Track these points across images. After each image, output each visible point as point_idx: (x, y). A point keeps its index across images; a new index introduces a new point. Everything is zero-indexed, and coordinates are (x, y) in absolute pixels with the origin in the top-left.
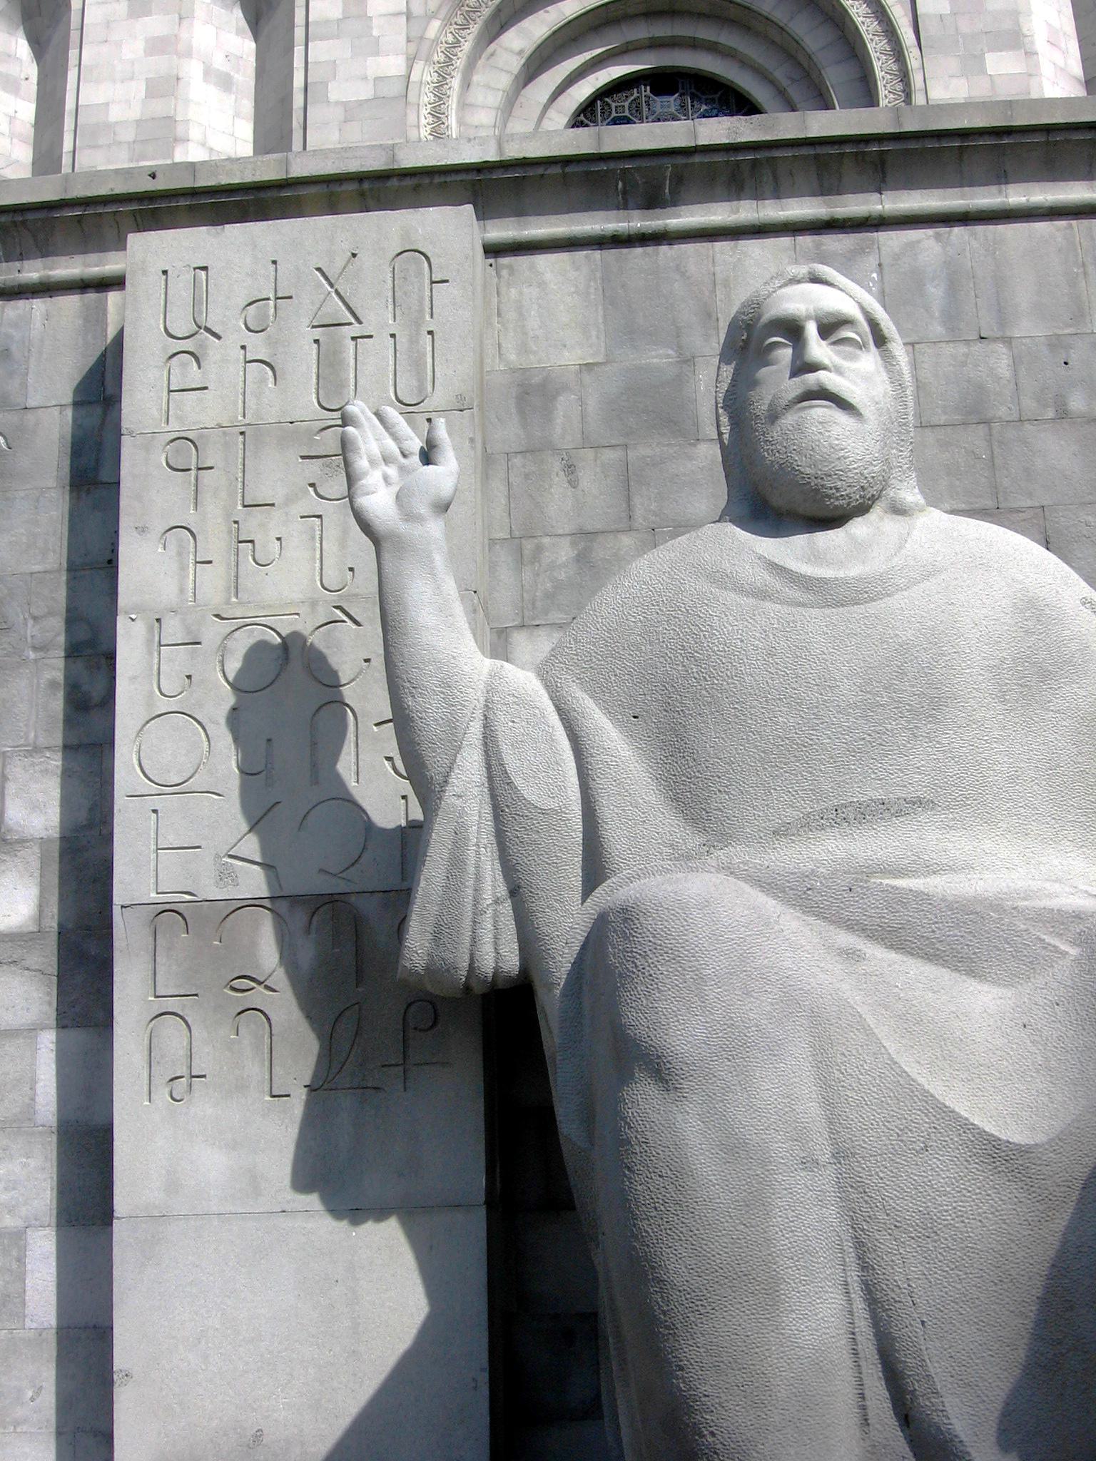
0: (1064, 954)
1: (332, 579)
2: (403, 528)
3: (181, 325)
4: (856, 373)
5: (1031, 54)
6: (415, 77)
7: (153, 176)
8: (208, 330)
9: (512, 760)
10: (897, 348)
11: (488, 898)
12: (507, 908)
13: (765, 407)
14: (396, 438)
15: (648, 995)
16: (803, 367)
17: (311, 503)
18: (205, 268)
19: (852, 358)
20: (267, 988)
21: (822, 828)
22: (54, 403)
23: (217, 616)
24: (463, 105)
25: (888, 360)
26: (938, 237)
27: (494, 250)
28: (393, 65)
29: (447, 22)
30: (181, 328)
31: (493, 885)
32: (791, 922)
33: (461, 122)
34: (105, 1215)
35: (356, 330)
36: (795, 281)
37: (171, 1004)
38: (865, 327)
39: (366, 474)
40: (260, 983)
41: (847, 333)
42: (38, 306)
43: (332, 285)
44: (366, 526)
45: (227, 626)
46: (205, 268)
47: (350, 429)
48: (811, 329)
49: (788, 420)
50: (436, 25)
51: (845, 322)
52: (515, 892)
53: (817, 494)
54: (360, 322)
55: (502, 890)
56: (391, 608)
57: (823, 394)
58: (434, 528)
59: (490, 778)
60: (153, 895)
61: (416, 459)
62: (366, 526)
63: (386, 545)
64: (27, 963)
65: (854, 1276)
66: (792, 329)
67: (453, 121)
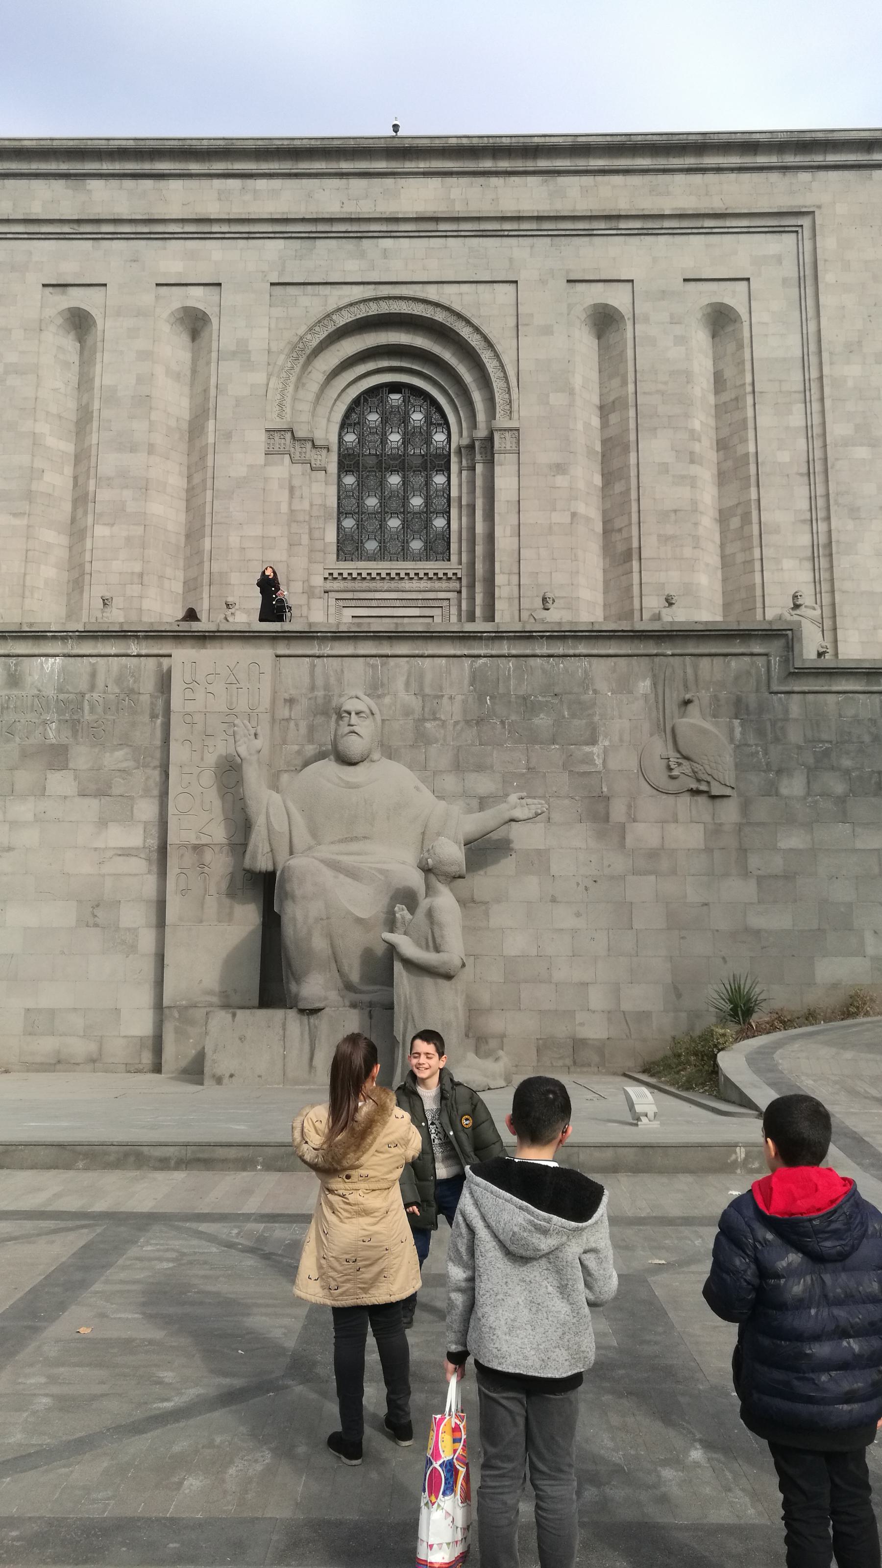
5: (572, 392)
6: (271, 385)
9: (272, 819)
24: (294, 399)
25: (374, 720)
26: (407, 662)
28: (260, 378)
29: (288, 356)
31: (267, 849)
32: (325, 869)
33: (293, 408)
35: (238, 686)
36: (352, 698)
37: (184, 871)
38: (368, 711)
48: (353, 714)
49: (345, 738)
50: (282, 357)
52: (272, 850)
55: (269, 850)
61: (253, 736)
67: (288, 410)
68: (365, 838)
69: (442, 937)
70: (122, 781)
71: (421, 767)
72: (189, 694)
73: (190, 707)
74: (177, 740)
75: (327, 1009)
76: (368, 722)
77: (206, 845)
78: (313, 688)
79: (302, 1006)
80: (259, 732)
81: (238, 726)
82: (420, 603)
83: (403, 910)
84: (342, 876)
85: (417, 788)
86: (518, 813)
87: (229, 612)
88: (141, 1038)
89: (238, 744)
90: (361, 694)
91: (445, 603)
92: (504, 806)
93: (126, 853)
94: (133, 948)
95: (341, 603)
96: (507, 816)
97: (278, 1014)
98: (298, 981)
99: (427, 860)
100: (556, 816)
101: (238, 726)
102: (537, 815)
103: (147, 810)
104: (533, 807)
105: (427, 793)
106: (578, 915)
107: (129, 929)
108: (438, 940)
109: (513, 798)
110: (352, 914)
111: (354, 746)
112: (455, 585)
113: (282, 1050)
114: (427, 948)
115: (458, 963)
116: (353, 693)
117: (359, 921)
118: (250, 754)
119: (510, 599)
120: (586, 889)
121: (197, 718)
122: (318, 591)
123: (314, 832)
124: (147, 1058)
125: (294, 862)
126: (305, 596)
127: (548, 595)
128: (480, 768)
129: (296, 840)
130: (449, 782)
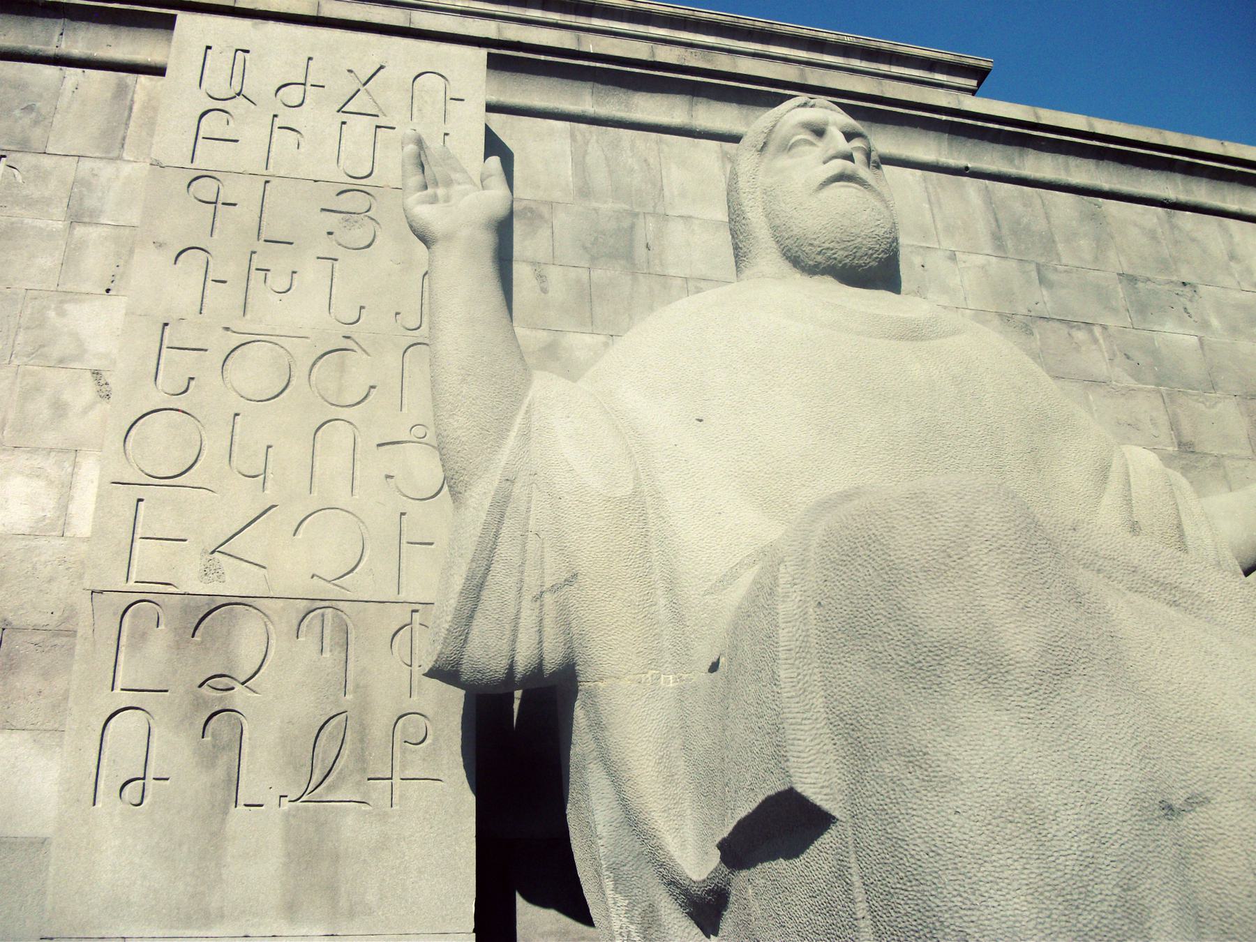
45: (236, 340)
78: (585, 192)
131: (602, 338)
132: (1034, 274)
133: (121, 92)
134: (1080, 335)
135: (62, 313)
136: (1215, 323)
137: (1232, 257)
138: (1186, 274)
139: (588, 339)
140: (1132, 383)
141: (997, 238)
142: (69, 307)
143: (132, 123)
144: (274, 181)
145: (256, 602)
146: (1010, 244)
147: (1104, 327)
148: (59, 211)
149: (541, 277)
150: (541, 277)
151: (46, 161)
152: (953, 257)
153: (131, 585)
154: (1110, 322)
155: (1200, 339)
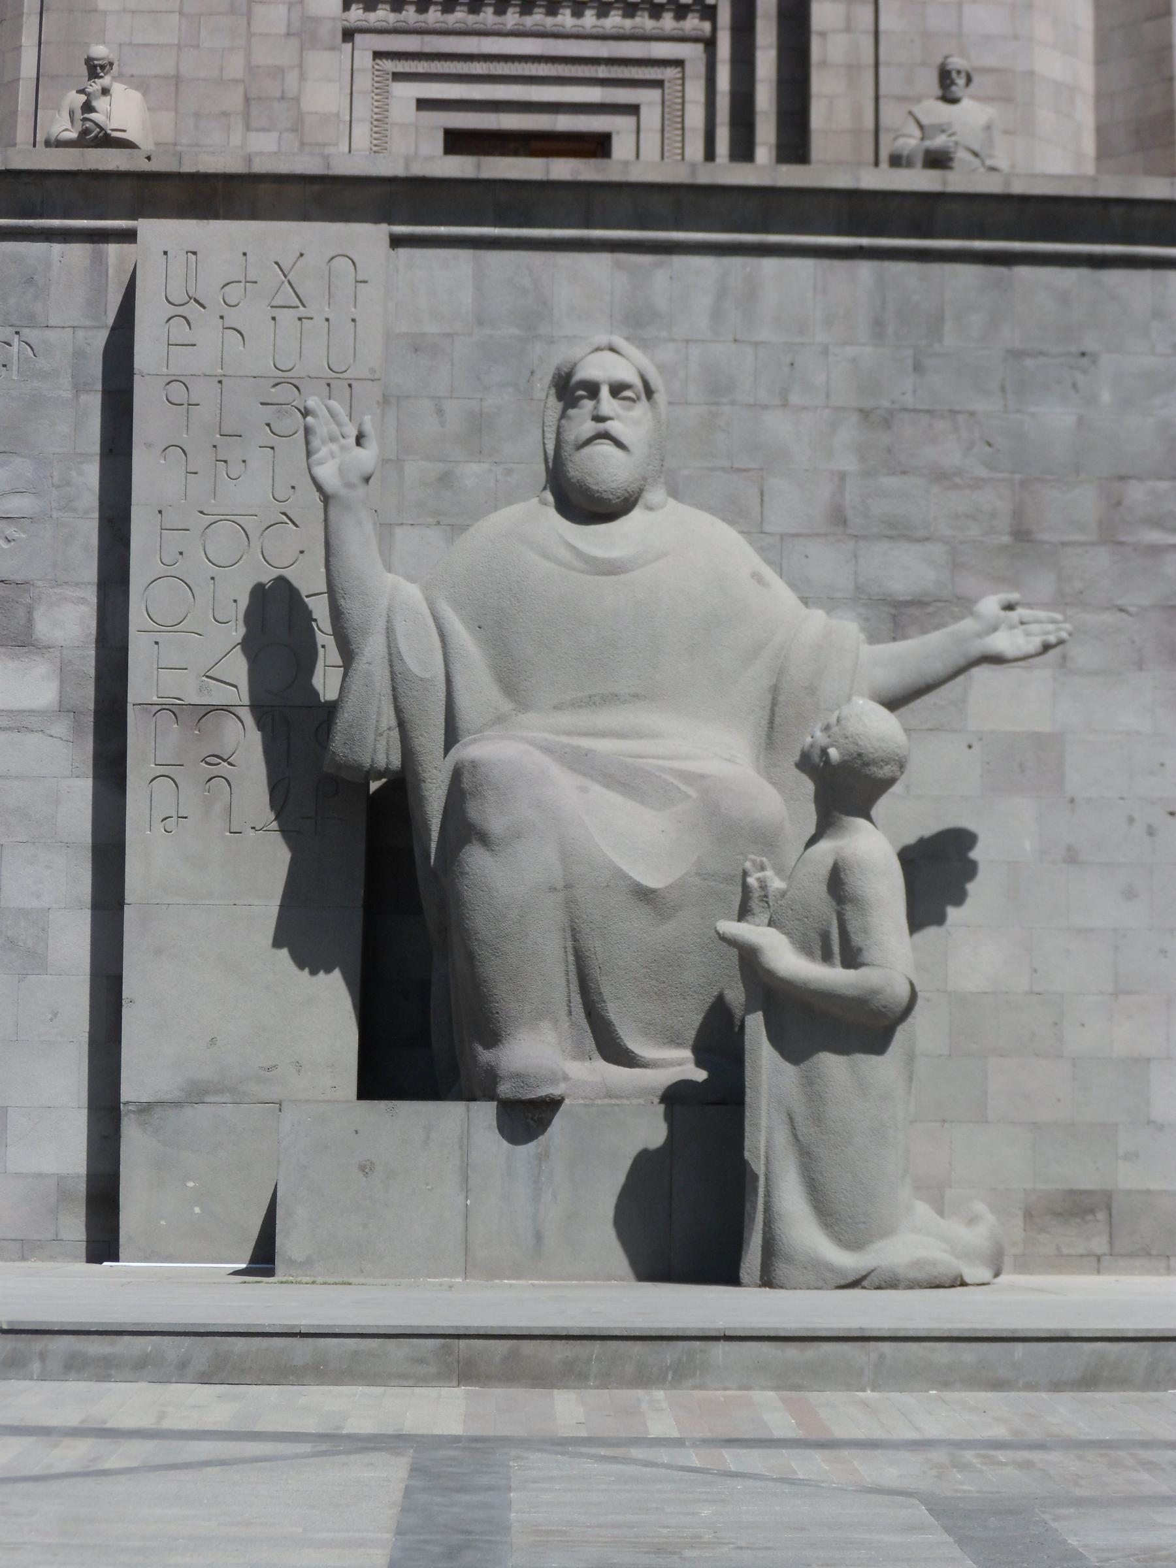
0: (689, 797)
1: (282, 493)
2: (343, 492)
3: (178, 296)
4: (630, 422)
7: (149, 158)
8: (196, 301)
9: (403, 645)
10: (661, 397)
11: (384, 726)
12: (395, 734)
13: (572, 437)
14: (339, 424)
15: (482, 804)
16: (599, 419)
17: (267, 437)
18: (195, 253)
19: (628, 409)
20: (229, 764)
21: (580, 707)
22: (69, 324)
23: (201, 512)
27: (397, 242)
30: (178, 296)
34: (120, 903)
36: (598, 349)
38: (639, 384)
39: (319, 450)
40: (224, 761)
41: (628, 393)
42: (57, 248)
43: (285, 276)
44: (319, 488)
46: (195, 253)
47: (309, 419)
48: (605, 392)
49: (587, 450)
51: (626, 386)
52: (401, 724)
53: (600, 501)
54: (304, 306)
55: (393, 722)
56: (334, 541)
57: (606, 436)
58: (361, 490)
59: (390, 654)
60: (155, 698)
61: (353, 440)
62: (319, 488)
63: (331, 501)
64: (52, 732)
65: (569, 944)
66: (593, 390)
68: (636, 696)
69: (865, 931)
70: (5, 546)
71: (751, 524)
72: (179, 331)
73: (182, 362)
74: (149, 445)
75: (567, 1101)
76: (641, 410)
77: (225, 709)
79: (505, 1089)
80: (368, 428)
81: (314, 415)
82: (602, 72)
83: (763, 868)
84: (596, 789)
85: (758, 578)
86: (1003, 642)
87: (95, 87)
88: (61, 1179)
89: (315, 457)
90: (619, 342)
91: (670, 73)
92: (967, 625)
93: (18, 722)
94: (34, 960)
95: (390, 66)
96: (977, 648)
97: (448, 1115)
98: (493, 1038)
99: (824, 752)
100: (1080, 654)
101: (314, 415)
102: (1046, 647)
103: (71, 621)
104: (1034, 628)
105: (779, 587)
106: (1130, 894)
107: (25, 913)
108: (857, 939)
109: (990, 605)
110: (626, 877)
111: (607, 468)
112: (693, 24)
113: (462, 1197)
114: (826, 957)
115: (903, 992)
116: (602, 339)
117: (644, 895)
118: (349, 485)
119: (852, 69)
120: (1151, 832)
121: (203, 391)
122: (330, 31)
123: (511, 681)
124: (75, 1227)
125: (469, 750)
126: (294, 43)
127: (956, 62)
128: (900, 531)
129: (464, 701)
130: (826, 562)
131: (486, 466)
132: (910, 362)
133: (99, 262)
134: (941, 425)
135: (81, 473)
136: (1106, 397)
137: (1158, 314)
138: (1090, 342)
139: (475, 467)
140: (983, 473)
141: (878, 325)
142: (85, 467)
143: (110, 290)
144: (225, 380)
145: (231, 709)
146: (890, 330)
147: (972, 414)
148: (66, 381)
149: (440, 412)
150: (440, 412)
151: (51, 335)
152: (825, 352)
153: (155, 699)
154: (982, 406)
155: (1081, 420)
